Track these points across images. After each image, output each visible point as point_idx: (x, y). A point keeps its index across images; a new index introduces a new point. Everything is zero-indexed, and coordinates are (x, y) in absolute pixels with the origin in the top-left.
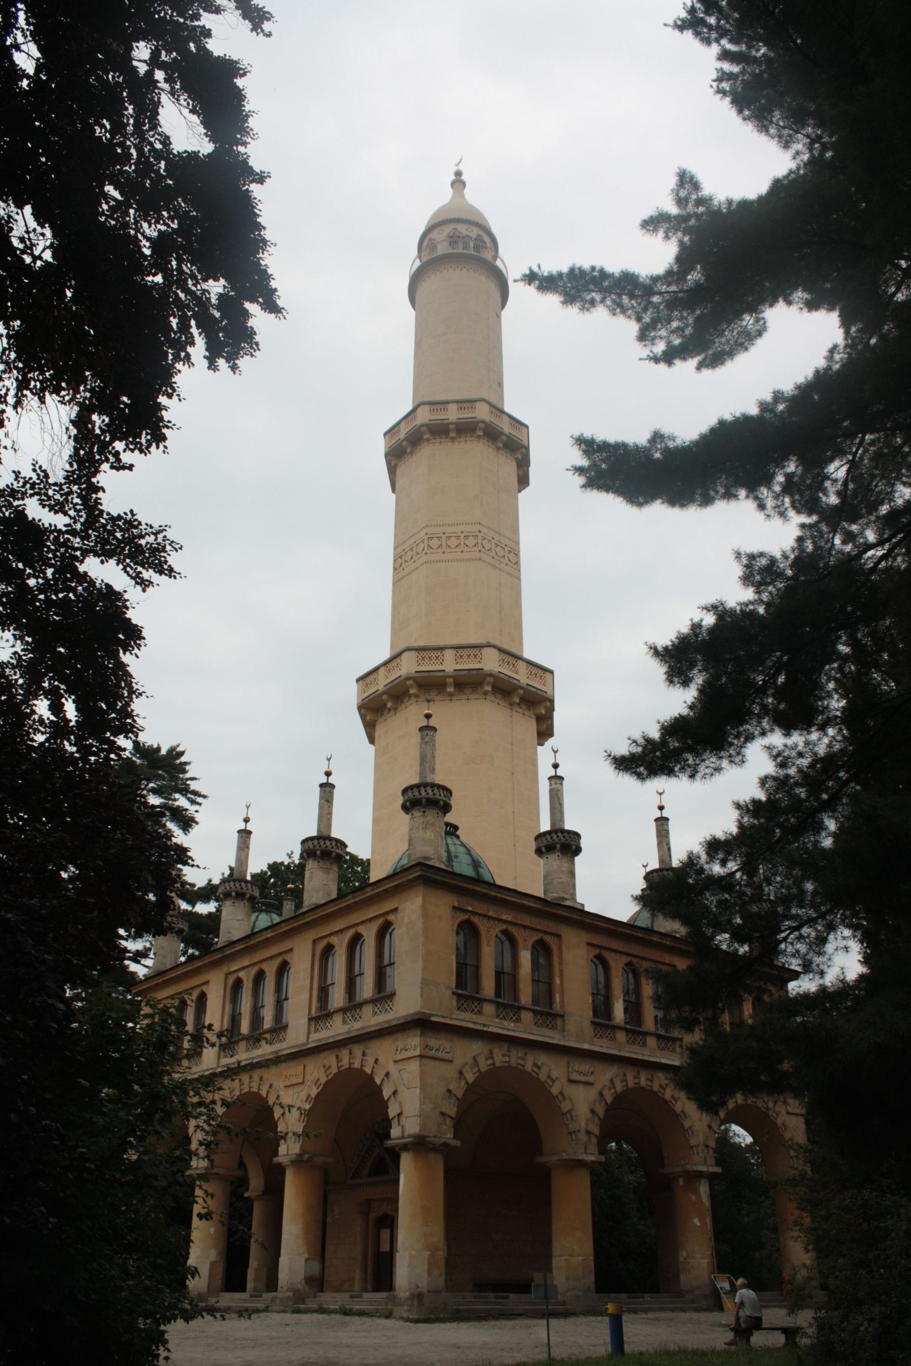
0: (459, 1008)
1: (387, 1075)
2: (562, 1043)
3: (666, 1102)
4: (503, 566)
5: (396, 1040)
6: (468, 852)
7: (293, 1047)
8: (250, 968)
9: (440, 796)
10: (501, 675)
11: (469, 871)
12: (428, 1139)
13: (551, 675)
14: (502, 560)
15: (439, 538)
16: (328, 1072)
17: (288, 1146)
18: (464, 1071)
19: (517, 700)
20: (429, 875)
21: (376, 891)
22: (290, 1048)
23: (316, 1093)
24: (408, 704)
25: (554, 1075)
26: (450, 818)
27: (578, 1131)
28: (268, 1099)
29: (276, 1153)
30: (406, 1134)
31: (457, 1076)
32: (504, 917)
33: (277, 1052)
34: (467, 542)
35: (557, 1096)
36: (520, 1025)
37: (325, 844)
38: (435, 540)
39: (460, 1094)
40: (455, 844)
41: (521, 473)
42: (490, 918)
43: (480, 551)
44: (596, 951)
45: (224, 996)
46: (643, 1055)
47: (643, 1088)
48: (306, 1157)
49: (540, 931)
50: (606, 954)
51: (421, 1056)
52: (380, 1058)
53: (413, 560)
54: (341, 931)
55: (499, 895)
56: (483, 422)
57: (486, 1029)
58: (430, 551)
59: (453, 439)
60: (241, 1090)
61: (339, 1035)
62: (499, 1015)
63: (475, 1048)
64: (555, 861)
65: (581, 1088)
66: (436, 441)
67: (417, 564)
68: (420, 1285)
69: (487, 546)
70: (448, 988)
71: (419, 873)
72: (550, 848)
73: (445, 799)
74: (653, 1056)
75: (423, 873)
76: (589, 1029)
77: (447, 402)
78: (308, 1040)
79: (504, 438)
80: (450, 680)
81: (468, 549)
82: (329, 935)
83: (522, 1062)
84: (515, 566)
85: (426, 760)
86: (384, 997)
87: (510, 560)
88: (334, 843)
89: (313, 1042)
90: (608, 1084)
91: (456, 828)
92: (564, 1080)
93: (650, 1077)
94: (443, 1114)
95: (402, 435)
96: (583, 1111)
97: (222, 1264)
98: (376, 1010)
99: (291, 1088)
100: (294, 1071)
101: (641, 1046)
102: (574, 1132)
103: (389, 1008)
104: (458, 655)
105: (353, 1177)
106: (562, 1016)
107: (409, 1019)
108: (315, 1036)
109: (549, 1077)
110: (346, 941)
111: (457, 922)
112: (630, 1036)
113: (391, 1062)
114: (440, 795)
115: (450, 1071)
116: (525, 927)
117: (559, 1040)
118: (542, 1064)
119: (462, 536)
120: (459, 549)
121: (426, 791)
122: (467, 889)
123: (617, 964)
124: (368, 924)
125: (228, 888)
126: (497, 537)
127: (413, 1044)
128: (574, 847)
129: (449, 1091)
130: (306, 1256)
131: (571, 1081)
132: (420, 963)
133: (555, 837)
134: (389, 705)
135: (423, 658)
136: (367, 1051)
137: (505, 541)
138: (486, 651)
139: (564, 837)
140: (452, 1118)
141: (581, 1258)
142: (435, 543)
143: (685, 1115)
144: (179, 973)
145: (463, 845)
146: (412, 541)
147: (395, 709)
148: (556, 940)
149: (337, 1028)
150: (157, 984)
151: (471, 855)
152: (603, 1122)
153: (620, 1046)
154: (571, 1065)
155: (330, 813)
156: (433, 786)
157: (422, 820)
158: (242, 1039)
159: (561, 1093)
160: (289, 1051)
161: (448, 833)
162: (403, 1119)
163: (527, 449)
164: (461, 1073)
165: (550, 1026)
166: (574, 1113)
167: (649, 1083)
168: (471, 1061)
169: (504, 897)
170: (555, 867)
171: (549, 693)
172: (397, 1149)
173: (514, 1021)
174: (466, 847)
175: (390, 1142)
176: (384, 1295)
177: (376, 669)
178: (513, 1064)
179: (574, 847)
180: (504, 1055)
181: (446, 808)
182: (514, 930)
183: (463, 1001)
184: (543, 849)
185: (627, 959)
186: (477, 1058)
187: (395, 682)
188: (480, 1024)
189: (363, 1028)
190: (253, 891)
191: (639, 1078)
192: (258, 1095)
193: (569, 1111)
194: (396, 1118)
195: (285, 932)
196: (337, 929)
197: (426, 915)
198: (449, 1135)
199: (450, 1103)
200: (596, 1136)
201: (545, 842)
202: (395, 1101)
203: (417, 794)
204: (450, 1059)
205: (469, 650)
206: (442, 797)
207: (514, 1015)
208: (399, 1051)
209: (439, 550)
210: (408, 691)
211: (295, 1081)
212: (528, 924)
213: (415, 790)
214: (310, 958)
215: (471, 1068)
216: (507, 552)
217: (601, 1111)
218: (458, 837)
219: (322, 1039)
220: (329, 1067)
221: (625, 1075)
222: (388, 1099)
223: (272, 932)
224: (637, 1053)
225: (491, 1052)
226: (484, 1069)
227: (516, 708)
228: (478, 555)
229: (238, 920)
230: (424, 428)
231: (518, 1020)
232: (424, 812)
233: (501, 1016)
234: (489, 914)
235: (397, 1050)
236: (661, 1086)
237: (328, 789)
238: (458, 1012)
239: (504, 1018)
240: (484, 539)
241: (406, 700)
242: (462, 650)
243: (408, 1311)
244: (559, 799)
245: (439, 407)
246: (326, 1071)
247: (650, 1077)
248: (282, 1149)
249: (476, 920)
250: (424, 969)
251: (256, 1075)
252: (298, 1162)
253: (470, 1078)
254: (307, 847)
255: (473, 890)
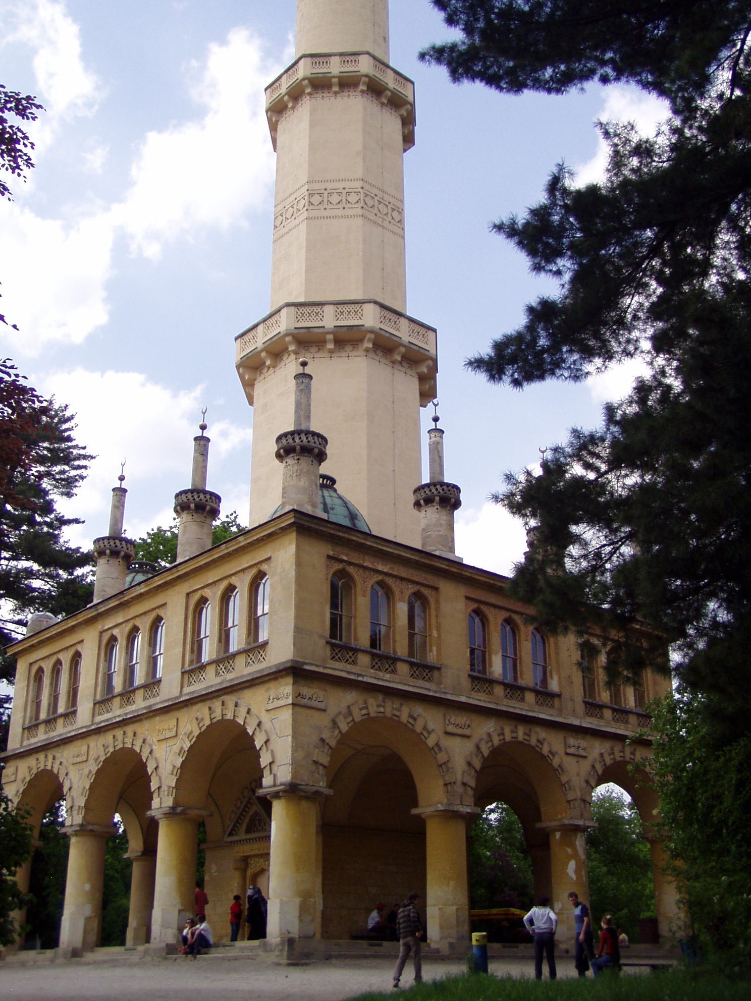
0: (332, 658)
1: (259, 724)
2: (437, 695)
3: (543, 757)
4: (386, 224)
5: (268, 689)
6: (345, 504)
8: (124, 625)
9: (313, 442)
10: (383, 333)
11: (346, 522)
12: (301, 787)
13: (434, 334)
14: (385, 217)
15: (320, 195)
16: (201, 725)
17: (161, 799)
18: (338, 720)
19: (399, 358)
20: (302, 522)
21: (249, 541)
22: (163, 702)
23: (189, 746)
24: (287, 361)
25: (431, 726)
26: (325, 468)
27: (454, 783)
28: (142, 754)
29: (149, 807)
30: (278, 782)
31: (331, 724)
32: (380, 567)
33: (151, 706)
34: (349, 198)
35: (433, 748)
36: (397, 677)
37: (199, 497)
38: (317, 196)
39: (333, 743)
40: (331, 497)
41: (406, 131)
42: (366, 568)
43: (362, 208)
44: (474, 606)
45: (99, 654)
46: (521, 709)
47: (521, 743)
48: (179, 809)
49: (417, 583)
50: (485, 609)
51: (293, 704)
52: (252, 710)
53: (293, 217)
54: (214, 583)
55: (375, 545)
56: (367, 76)
57: (360, 679)
58: (311, 207)
59: (336, 93)
60: (115, 747)
61: (212, 686)
62: (374, 666)
63: (350, 697)
64: (432, 514)
65: (458, 740)
66: (317, 95)
67: (297, 221)
68: (291, 930)
69: (370, 203)
70: (321, 636)
71: (292, 520)
72: (429, 501)
73: (320, 446)
74: (530, 711)
75: (299, 521)
76: (466, 683)
77: (329, 55)
78: (181, 693)
79: (389, 93)
80: (330, 337)
81: (350, 206)
82: (202, 588)
83: (397, 713)
84: (398, 224)
85: (303, 408)
86: (257, 647)
87: (393, 218)
88: (208, 497)
89: (185, 694)
90: (485, 737)
91: (333, 481)
92: (441, 733)
93: (527, 731)
94: (315, 762)
95: (283, 90)
96: (459, 764)
97: (96, 921)
98: (249, 660)
99: (164, 742)
100: (166, 724)
101: (519, 701)
102: (450, 783)
103: (262, 658)
104: (338, 311)
105: (230, 834)
106: (439, 669)
107: (282, 667)
108: (187, 690)
109: (425, 728)
110: (219, 593)
111: (332, 571)
112: (508, 690)
113: (264, 712)
114: (315, 443)
115: (323, 720)
116: (402, 579)
117: (436, 692)
118: (418, 716)
119: (344, 192)
121: (300, 438)
122: (342, 538)
123: (496, 619)
124: (241, 574)
125: (102, 546)
126: (380, 194)
127: (285, 692)
128: (453, 500)
129: (323, 740)
130: (179, 907)
131: (447, 733)
132: (292, 612)
133: (434, 490)
134: (268, 363)
135: (303, 314)
136: (239, 702)
137: (388, 198)
138: (365, 306)
139: (443, 490)
140: (325, 767)
141: (454, 908)
142: (316, 199)
143: (562, 770)
144: (54, 633)
145: (340, 497)
146: (293, 197)
147: (274, 367)
148: (434, 593)
149: (210, 680)
150: (32, 646)
151: (347, 507)
152: (480, 774)
153: (499, 700)
154: (448, 718)
155: (205, 467)
156: (308, 433)
157: (296, 467)
158: (116, 696)
159: (437, 745)
160: (162, 706)
161: (323, 486)
162: (275, 768)
163: (413, 105)
164: (334, 722)
165: (427, 678)
166: (450, 765)
167: (526, 737)
168: (344, 711)
169: (380, 547)
170: (434, 520)
171: (432, 351)
172: (268, 797)
173: (390, 672)
174: (343, 500)
175: (261, 791)
176: (256, 943)
177: (255, 326)
178: (388, 714)
179: (453, 500)
180: (378, 706)
181: (321, 457)
182: (390, 581)
183: (337, 651)
184: (422, 502)
185: (505, 615)
186: (352, 708)
187: (273, 340)
188: (354, 674)
189: (237, 678)
190: (127, 549)
191: (516, 732)
192: (131, 751)
193: (444, 763)
194: (268, 767)
195: (159, 586)
196: (210, 582)
197: (299, 564)
198: (321, 784)
199: (323, 752)
200: (472, 788)
201: (424, 495)
202: (267, 751)
203: (291, 441)
204: (324, 708)
205: (349, 306)
206: (317, 445)
207: (390, 666)
208: (271, 700)
209: (320, 206)
210: (288, 348)
212: (404, 575)
213: (289, 436)
214: (184, 612)
215: (345, 718)
216: (390, 210)
217: (477, 764)
218: (335, 490)
219: (193, 692)
220: (202, 719)
221: (502, 729)
222: (260, 749)
223: (146, 586)
224: (514, 708)
225: (365, 702)
226: (358, 718)
227: (398, 366)
228: (360, 212)
229: (113, 578)
230: (306, 82)
231: (394, 672)
232: (298, 459)
233: (377, 667)
234: (365, 564)
235: (269, 699)
236: (538, 741)
237: (202, 443)
238: (332, 662)
239: (379, 669)
240: (366, 195)
241: (286, 356)
242: (342, 306)
243: (277, 956)
244: (438, 452)
245: (321, 60)
246: (198, 724)
247: (527, 731)
248: (155, 803)
249: (351, 570)
250: (297, 617)
251: (130, 729)
252: (172, 813)
253: (344, 727)
254: (181, 501)
255: (348, 540)
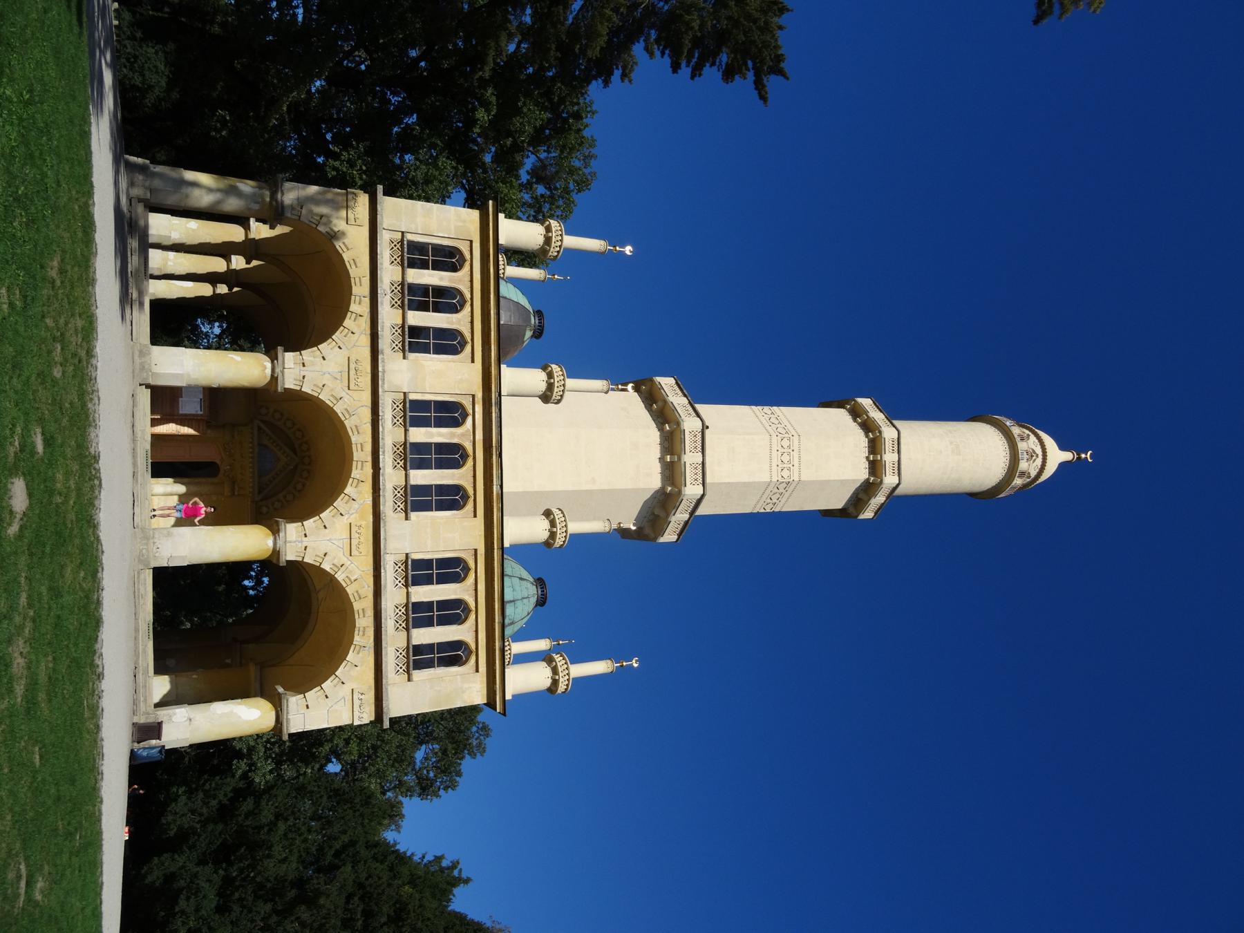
7: (385, 543)
54: (476, 590)
105: (260, 428)
120: (780, 448)
136: (367, 648)
211: (354, 542)
235: (362, 694)
